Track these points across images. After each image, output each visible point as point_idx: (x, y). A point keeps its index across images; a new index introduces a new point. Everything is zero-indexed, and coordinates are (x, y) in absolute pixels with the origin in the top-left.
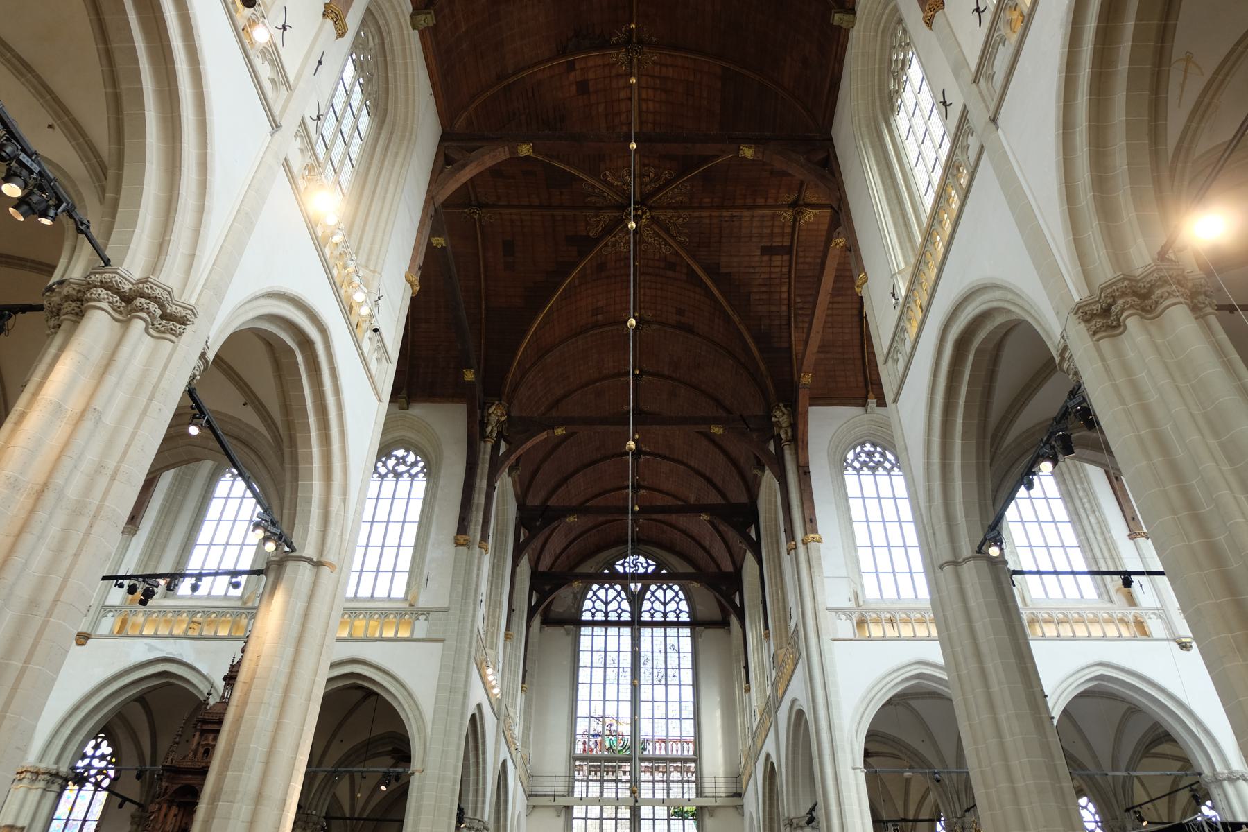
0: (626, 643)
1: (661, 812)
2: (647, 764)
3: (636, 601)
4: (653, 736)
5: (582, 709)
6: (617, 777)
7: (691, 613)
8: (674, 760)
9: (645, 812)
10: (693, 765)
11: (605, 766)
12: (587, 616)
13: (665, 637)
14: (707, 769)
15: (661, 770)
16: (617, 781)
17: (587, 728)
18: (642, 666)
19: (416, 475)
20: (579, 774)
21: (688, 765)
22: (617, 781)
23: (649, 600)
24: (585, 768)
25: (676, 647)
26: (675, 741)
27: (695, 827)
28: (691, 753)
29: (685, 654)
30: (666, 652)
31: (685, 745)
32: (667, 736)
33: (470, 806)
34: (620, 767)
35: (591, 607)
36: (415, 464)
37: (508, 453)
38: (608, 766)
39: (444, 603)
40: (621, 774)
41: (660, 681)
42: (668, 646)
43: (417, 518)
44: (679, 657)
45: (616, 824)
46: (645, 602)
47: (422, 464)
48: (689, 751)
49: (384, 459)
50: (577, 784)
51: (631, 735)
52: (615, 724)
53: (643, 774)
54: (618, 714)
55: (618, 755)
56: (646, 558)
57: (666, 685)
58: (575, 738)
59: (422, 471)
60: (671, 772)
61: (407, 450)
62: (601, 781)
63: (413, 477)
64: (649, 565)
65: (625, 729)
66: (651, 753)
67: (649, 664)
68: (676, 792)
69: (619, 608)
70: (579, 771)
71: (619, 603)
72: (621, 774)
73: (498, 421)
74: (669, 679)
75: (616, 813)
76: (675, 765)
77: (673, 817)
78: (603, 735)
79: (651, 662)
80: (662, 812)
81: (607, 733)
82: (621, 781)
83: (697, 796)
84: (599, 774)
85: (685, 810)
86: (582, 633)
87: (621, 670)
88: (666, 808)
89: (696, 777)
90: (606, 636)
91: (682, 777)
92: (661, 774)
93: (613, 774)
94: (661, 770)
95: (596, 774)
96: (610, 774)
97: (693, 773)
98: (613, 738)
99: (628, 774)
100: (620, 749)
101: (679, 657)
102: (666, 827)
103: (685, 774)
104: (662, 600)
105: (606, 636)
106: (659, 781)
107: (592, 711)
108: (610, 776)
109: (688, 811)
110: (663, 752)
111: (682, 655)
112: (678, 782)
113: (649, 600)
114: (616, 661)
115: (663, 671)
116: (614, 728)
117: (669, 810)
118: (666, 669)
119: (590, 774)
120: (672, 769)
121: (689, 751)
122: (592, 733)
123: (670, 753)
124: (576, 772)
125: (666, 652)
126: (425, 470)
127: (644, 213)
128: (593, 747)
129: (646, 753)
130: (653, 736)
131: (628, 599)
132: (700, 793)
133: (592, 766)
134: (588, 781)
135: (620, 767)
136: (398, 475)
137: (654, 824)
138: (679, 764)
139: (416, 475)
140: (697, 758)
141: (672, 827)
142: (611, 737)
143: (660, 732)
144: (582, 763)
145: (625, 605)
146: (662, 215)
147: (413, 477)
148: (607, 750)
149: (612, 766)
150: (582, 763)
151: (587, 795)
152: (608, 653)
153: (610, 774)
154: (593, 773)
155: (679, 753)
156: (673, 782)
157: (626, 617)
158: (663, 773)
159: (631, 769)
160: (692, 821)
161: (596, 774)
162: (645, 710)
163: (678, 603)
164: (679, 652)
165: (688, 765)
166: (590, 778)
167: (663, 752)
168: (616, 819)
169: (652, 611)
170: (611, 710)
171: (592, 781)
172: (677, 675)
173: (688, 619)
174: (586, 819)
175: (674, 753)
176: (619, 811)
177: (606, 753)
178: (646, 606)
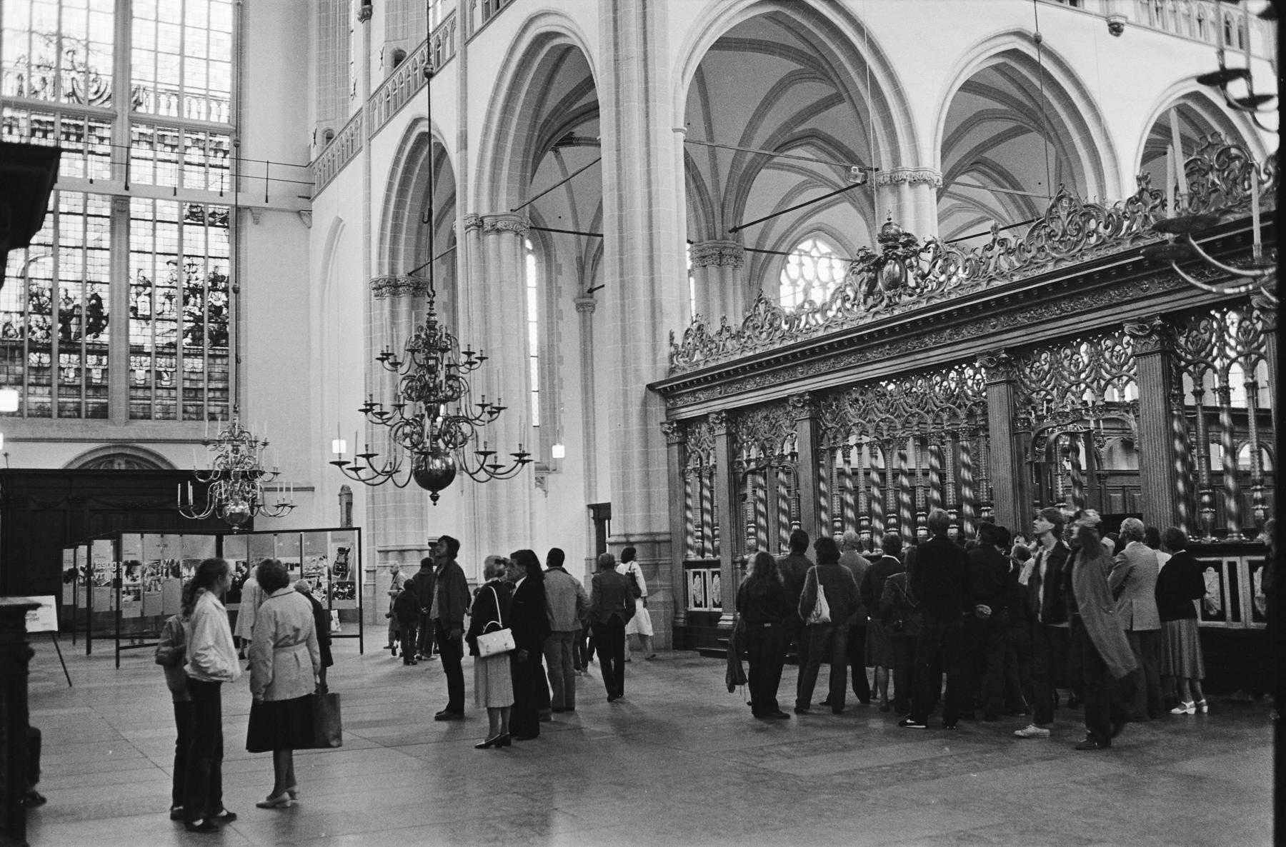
2: (143, 129)
4: (156, 82)
8: (193, 129)
9: (138, 207)
11: (63, 124)
14: (252, 148)
15: (168, 141)
17: (26, 52)
20: (10, 132)
21: (218, 139)
24: (23, 123)
26: (197, 96)
28: (224, 120)
31: (214, 104)
32: (181, 85)
34: (91, 129)
45: (86, 223)
48: (222, 115)
54: (88, 33)
55: (85, 107)
65: (103, 64)
66: (151, 111)
68: (194, 179)
75: (85, 207)
76: (195, 137)
77: (188, 221)
78: (58, 69)
80: (170, 210)
88: (176, 204)
93: (78, 140)
94: (168, 141)
95: (45, 136)
96: (73, 138)
98: (78, 76)
100: (92, 97)
102: (176, 235)
103: (212, 153)
107: (35, 22)
110: (174, 113)
116: (80, 57)
117: (181, 209)
121: (222, 115)
122: (35, 61)
123: (186, 116)
129: (140, 109)
130: (156, 82)
133: (39, 122)
137: (154, 229)
138: (201, 136)
140: (236, 131)
141: (186, 236)
143: (169, 77)
144: (16, 114)
148: (68, 96)
150: (16, 114)
153: (73, 138)
154: (39, 134)
155: (203, 117)
158: (173, 147)
159: (114, 134)
175: (194, 116)
177: (64, 101)
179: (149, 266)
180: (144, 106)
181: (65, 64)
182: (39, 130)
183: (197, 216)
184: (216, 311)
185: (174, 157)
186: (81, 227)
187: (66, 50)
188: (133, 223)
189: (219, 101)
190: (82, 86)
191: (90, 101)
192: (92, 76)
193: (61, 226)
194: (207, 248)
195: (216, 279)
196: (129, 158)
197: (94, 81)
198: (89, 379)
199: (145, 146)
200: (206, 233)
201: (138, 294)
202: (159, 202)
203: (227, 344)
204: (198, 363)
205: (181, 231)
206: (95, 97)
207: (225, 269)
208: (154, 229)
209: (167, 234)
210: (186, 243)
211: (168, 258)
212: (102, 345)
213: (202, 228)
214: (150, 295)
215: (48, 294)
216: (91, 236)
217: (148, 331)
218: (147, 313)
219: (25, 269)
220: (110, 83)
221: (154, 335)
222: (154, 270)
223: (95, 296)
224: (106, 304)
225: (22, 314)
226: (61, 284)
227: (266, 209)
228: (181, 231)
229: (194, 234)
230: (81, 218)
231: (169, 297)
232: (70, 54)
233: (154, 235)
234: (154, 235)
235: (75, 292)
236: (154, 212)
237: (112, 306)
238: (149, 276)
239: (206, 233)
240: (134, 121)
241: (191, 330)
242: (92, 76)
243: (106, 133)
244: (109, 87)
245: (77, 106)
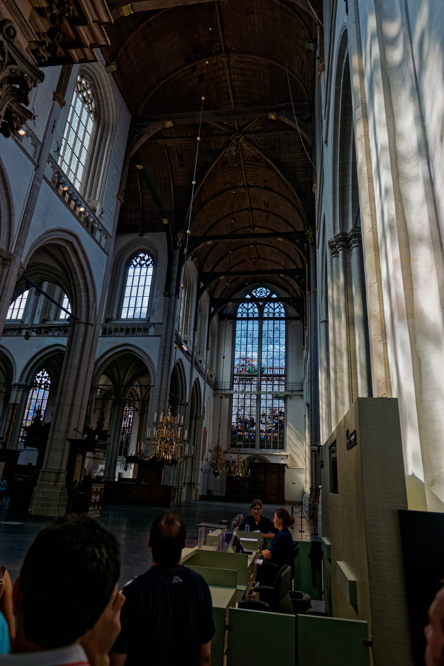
0: (256, 327)
1: (269, 397)
2: (264, 378)
3: (261, 309)
4: (267, 366)
5: (237, 355)
6: (251, 383)
7: (286, 313)
8: (276, 376)
9: (263, 396)
10: (284, 378)
11: (246, 378)
12: (239, 316)
13: (274, 324)
15: (270, 380)
16: (251, 384)
19: (149, 265)
21: (282, 378)
22: (251, 384)
23: (267, 307)
24: (238, 379)
25: (278, 328)
26: (277, 368)
27: (283, 403)
28: (283, 373)
29: (282, 332)
30: (274, 331)
31: (281, 370)
33: (180, 396)
34: (252, 379)
35: (241, 311)
36: (148, 260)
37: (188, 253)
38: (247, 378)
39: (161, 321)
40: (253, 381)
41: (271, 343)
42: (275, 328)
43: (150, 284)
44: (280, 333)
45: (251, 401)
46: (265, 309)
47: (151, 260)
48: (282, 372)
49: (135, 258)
50: (234, 385)
51: (257, 366)
52: (251, 361)
53: (262, 382)
54: (252, 357)
55: (251, 374)
56: (266, 289)
57: (273, 345)
58: (234, 367)
59: (151, 263)
60: (274, 381)
61: (145, 254)
62: (245, 384)
63: (148, 266)
64: (267, 292)
65: (255, 363)
66: (266, 373)
67: (266, 336)
69: (254, 311)
70: (235, 380)
71: (254, 309)
72: (253, 381)
73: (182, 239)
74: (275, 342)
75: (251, 397)
76: (276, 378)
78: (246, 366)
79: (267, 335)
80: (270, 397)
81: (247, 365)
82: (253, 384)
83: (285, 391)
84: (244, 381)
85: (280, 396)
86: (237, 323)
87: (254, 338)
88: (272, 395)
89: (285, 383)
90: (247, 324)
91: (279, 383)
92: (270, 382)
94: (270, 380)
95: (242, 381)
96: (248, 381)
101: (280, 333)
102: (271, 402)
104: (273, 307)
105: (247, 324)
106: (269, 385)
107: (241, 356)
108: (248, 382)
109: (281, 396)
110: (271, 373)
111: (281, 332)
112: (277, 385)
113: (267, 307)
114: (252, 335)
115: (272, 339)
116: (250, 363)
117: (273, 396)
118: (274, 338)
119: (240, 381)
120: (275, 380)
122: (241, 364)
124: (234, 381)
125: (274, 331)
126: (153, 263)
127: (241, 137)
128: (241, 370)
129: (264, 373)
131: (257, 307)
132: (286, 390)
133: (241, 378)
134: (239, 384)
135: (252, 379)
136: (141, 265)
137: (266, 401)
138: (278, 378)
139: (149, 265)
141: (274, 402)
142: (249, 366)
143: (270, 365)
145: (256, 310)
146: (250, 136)
147: (148, 266)
148: (247, 372)
149: (249, 378)
150: (237, 377)
151: (239, 390)
152: (248, 331)
153: (248, 381)
154: (241, 381)
155: (278, 373)
156: (275, 385)
157: (256, 315)
160: (282, 401)
161: (242, 381)
162: (264, 355)
163: (280, 309)
164: (280, 331)
165: (282, 378)
166: (240, 383)
167: (271, 373)
168: (251, 399)
169: (268, 313)
170: (249, 355)
171: (241, 384)
172: (278, 340)
173: (284, 316)
174: (238, 399)
175: (276, 373)
176: (252, 396)
177: (247, 373)
178: (266, 310)
179: (265, 410)
181: (247, 365)
183: (277, 397)
184: (281, 421)
185: (271, 383)
186: (250, 402)
188: (262, 400)
189: (282, 369)
191: (252, 372)
192: (253, 367)
193: (246, 402)
194: (279, 405)
195: (281, 413)
196: (261, 384)
198: (251, 438)
199: (264, 382)
200: (279, 402)
201: (262, 418)
202: (268, 395)
203: (284, 429)
204: (276, 435)
205: (273, 402)
207: (283, 410)
208: (266, 401)
209: (269, 402)
210: (274, 404)
211: (269, 408)
212: (254, 430)
213: (278, 400)
214: (265, 418)
215: (242, 418)
216: (252, 404)
217: (265, 426)
218: (264, 422)
219: (238, 413)
221: (266, 427)
222: (266, 411)
223: (253, 419)
224: (255, 420)
225: (236, 423)
226: (245, 416)
227: (293, 395)
228: (273, 402)
229: (276, 402)
230: (250, 400)
231: (269, 418)
233: (266, 403)
234: (266, 403)
235: (248, 418)
236: (267, 397)
237: (256, 421)
238: (265, 412)
239: (279, 402)
240: (261, 376)
241: (275, 426)
242: (253, 367)
243: (256, 379)
245: (250, 374)
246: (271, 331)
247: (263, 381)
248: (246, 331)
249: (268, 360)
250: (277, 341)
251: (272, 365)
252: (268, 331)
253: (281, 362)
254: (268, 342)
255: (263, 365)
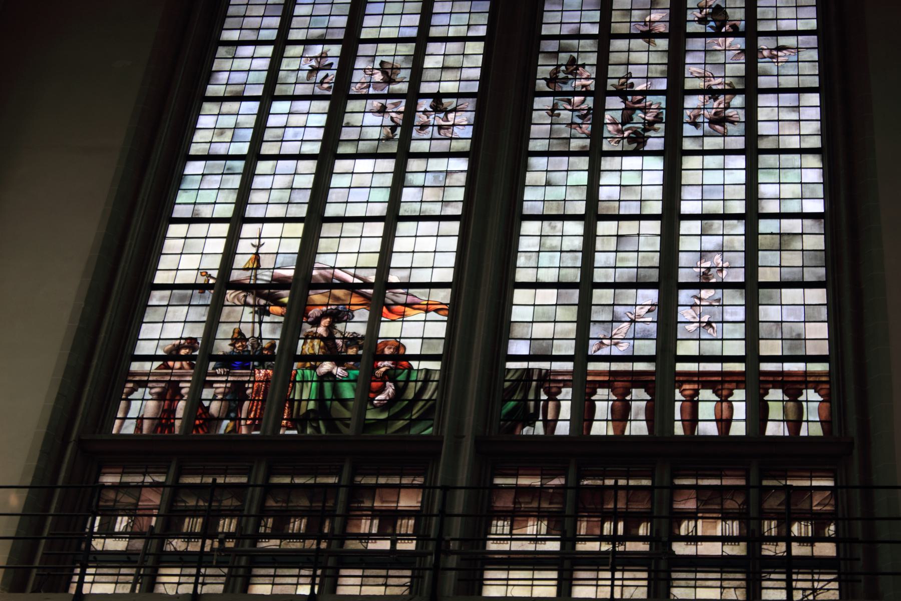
4: (582, 356)
17: (198, 332)
18: (541, 85)
28: (811, 428)
31: (775, 395)
34: (357, 492)
52: (362, 314)
53: (500, 527)
67: (586, 79)
70: (110, 515)
79: (591, 72)
87: (425, 104)
97: (819, 520)
98: (339, 371)
99: (407, 525)
111: (763, 43)
114: (405, 74)
116: (357, 327)
122: (223, 346)
123: (679, 429)
164: (751, 33)
180: (539, 425)
182: (194, 513)
187: (314, 312)
190: (348, 392)
197: (389, 376)
206: (384, 416)
220: (436, 377)
232: (325, 322)
242: (384, 365)
244: (432, 386)
246: (649, 35)
247: (515, 516)
248: (335, 50)
249: (601, 296)
250: (720, 120)
251: (649, 348)
252: (605, 37)
253: (768, 313)
254: (596, 136)
255: (518, 348)
